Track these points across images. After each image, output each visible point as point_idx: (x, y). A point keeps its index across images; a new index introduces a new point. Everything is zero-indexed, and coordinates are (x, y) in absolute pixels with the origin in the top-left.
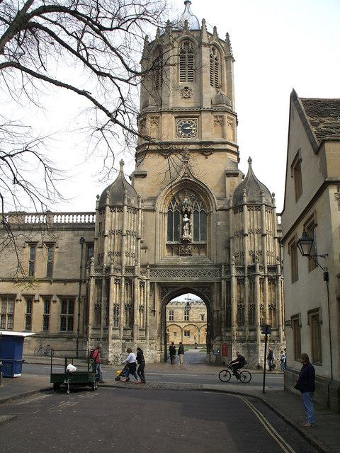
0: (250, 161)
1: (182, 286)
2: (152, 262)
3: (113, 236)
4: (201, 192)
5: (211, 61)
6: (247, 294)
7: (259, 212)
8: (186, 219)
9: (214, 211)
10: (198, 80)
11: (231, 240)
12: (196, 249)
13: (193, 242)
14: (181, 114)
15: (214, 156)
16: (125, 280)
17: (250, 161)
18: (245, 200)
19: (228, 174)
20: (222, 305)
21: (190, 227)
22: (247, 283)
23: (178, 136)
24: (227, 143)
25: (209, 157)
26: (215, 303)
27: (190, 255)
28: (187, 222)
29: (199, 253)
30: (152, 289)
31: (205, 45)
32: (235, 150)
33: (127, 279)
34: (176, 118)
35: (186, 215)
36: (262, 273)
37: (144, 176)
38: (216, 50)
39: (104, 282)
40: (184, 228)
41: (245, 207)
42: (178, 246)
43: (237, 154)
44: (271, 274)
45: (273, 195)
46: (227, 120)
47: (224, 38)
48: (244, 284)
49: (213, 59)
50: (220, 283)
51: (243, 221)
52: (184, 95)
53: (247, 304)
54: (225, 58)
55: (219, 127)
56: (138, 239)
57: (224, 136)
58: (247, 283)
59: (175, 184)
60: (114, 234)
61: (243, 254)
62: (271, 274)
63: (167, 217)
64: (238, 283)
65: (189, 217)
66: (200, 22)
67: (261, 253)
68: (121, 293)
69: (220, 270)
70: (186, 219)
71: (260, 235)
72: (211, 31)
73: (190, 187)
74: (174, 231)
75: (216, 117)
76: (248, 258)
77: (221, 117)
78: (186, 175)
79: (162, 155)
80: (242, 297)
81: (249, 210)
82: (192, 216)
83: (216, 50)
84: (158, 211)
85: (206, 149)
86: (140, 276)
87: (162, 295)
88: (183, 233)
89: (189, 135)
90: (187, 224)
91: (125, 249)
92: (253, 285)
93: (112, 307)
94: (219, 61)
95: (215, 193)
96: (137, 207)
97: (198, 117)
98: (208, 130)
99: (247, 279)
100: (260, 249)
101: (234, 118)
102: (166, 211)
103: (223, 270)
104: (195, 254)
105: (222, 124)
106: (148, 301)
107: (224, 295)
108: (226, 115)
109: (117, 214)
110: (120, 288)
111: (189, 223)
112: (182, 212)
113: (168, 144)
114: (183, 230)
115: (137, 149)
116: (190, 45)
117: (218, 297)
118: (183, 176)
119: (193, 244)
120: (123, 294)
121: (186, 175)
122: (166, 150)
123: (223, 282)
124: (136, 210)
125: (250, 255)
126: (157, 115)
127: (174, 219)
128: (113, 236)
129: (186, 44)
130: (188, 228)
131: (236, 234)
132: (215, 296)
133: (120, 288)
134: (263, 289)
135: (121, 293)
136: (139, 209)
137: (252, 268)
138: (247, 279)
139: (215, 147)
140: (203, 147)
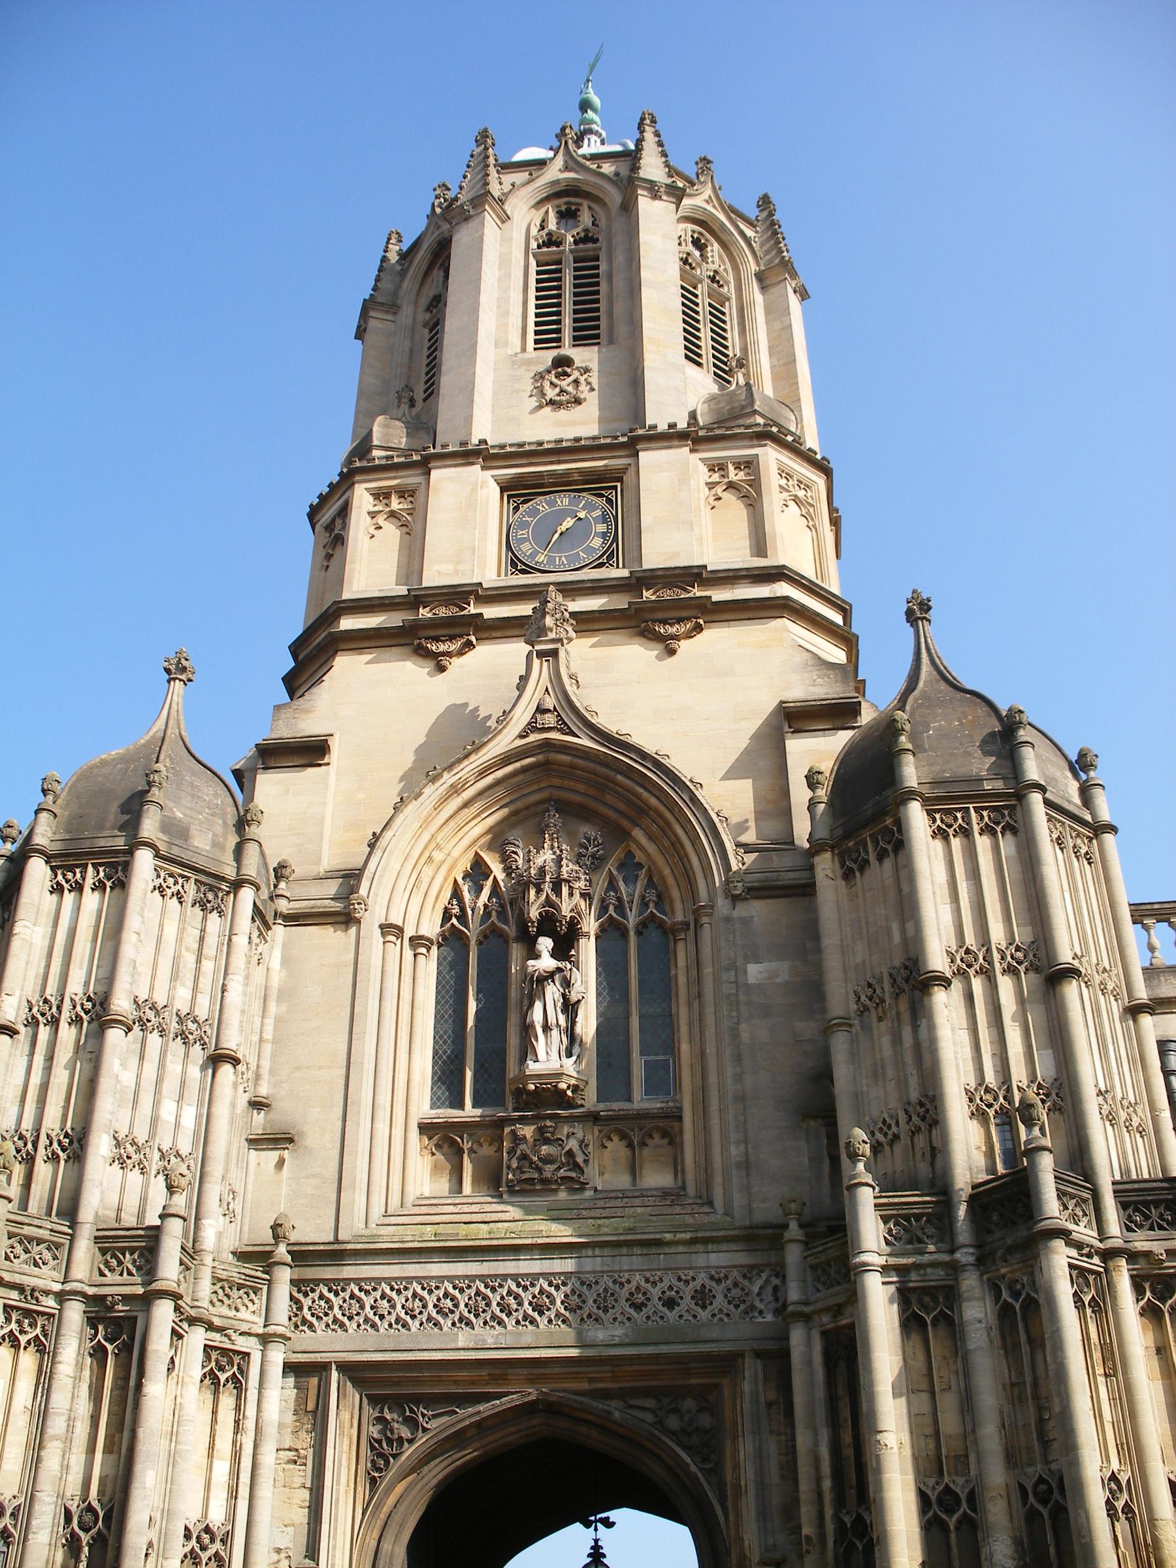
0: (918, 611)
2: (312, 1229)
3: (44, 1033)
4: (640, 812)
6: (989, 1398)
8: (546, 962)
9: (722, 904)
10: (622, 330)
11: (840, 1044)
12: (616, 1146)
14: (528, 479)
15: (716, 639)
16: (92, 1321)
17: (918, 611)
18: (911, 773)
19: (796, 718)
20: (806, 1512)
21: (570, 1008)
22: (977, 1312)
23: (516, 564)
24: (779, 574)
25: (684, 646)
26: (749, 1505)
27: (577, 1185)
28: (551, 975)
29: (634, 1170)
30: (314, 1416)
31: (654, 190)
32: (838, 619)
33: (99, 1311)
34: (506, 487)
35: (545, 944)
36: (1084, 1232)
37: (312, 752)
38: (714, 248)
40: (537, 1015)
41: (917, 816)
42: (493, 1115)
44: (1142, 1242)
45: (1082, 764)
46: (771, 480)
48: (951, 1325)
50: (777, 1359)
51: (906, 905)
52: (551, 393)
53: (996, 1475)
54: (760, 277)
55: (735, 510)
56: (217, 1059)
57: (760, 546)
58: (977, 1312)
59: (483, 773)
60: (54, 1022)
61: (928, 1111)
62: (1142, 1242)
63: (429, 967)
64: (910, 1323)
67: (1064, 1093)
68: (41, 1416)
69: (780, 1271)
70: (546, 962)
73: (583, 789)
74: (479, 1049)
75: (717, 467)
76: (969, 1150)
77: (749, 465)
78: (550, 720)
79: (422, 653)
80: (950, 1423)
81: (940, 834)
82: (587, 950)
83: (714, 248)
84: (372, 919)
86: (219, 1313)
87: (379, 1456)
88: (527, 1050)
90: (553, 991)
91: (111, 1114)
92: (1025, 1321)
95: (730, 801)
96: (230, 872)
97: (617, 476)
98: (681, 516)
99: (970, 1282)
100: (1045, 1068)
102: (431, 927)
103: (793, 1255)
104: (606, 1170)
105: (751, 495)
106: (265, 1491)
107: (812, 1441)
108: (771, 457)
109: (91, 900)
110: (45, 1381)
111: (567, 983)
112: (522, 922)
113: (458, 594)
114: (527, 1030)
115: (296, 648)
116: (586, 219)
117: (773, 1449)
118: (532, 727)
119: (594, 1118)
120: (56, 1425)
121: (550, 720)
122: (432, 624)
123: (797, 1336)
124: (214, 889)
125: (979, 1114)
126: (411, 479)
127: (487, 955)
128: (44, 1033)
129: (567, 215)
130: (558, 1018)
131: (870, 1002)
132: (746, 1448)
133: (45, 1381)
134: (1112, 1360)
135: (41, 1416)
136: (237, 885)
137: (1008, 1201)
138: (970, 1282)
139: (720, 595)
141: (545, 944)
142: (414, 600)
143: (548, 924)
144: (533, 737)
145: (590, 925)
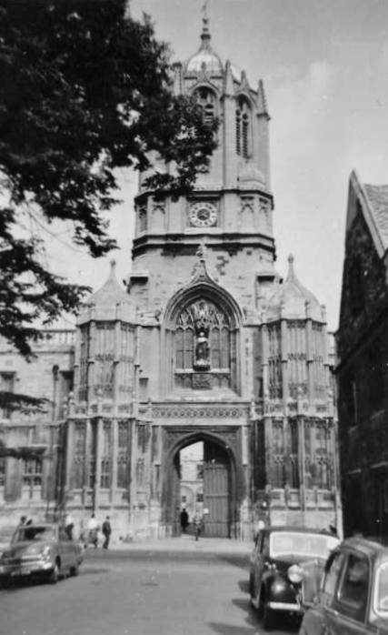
0: (291, 260)
1: (197, 431)
5: (238, 120)
7: (303, 331)
13: (213, 370)
16: (119, 423)
17: (291, 260)
39: (89, 426)
43: (272, 250)
47: (255, 87)
49: (241, 117)
65: (206, 336)
66: (224, 64)
69: (249, 409)
71: (304, 362)
72: (238, 78)
85: (231, 245)
89: (206, 223)
93: (99, 461)
94: (249, 120)
101: (269, 201)
139: (242, 241)
140: (227, 241)
141: (202, 334)
142: (166, 237)
143: (202, 329)
144: (200, 283)
145: (211, 329)
